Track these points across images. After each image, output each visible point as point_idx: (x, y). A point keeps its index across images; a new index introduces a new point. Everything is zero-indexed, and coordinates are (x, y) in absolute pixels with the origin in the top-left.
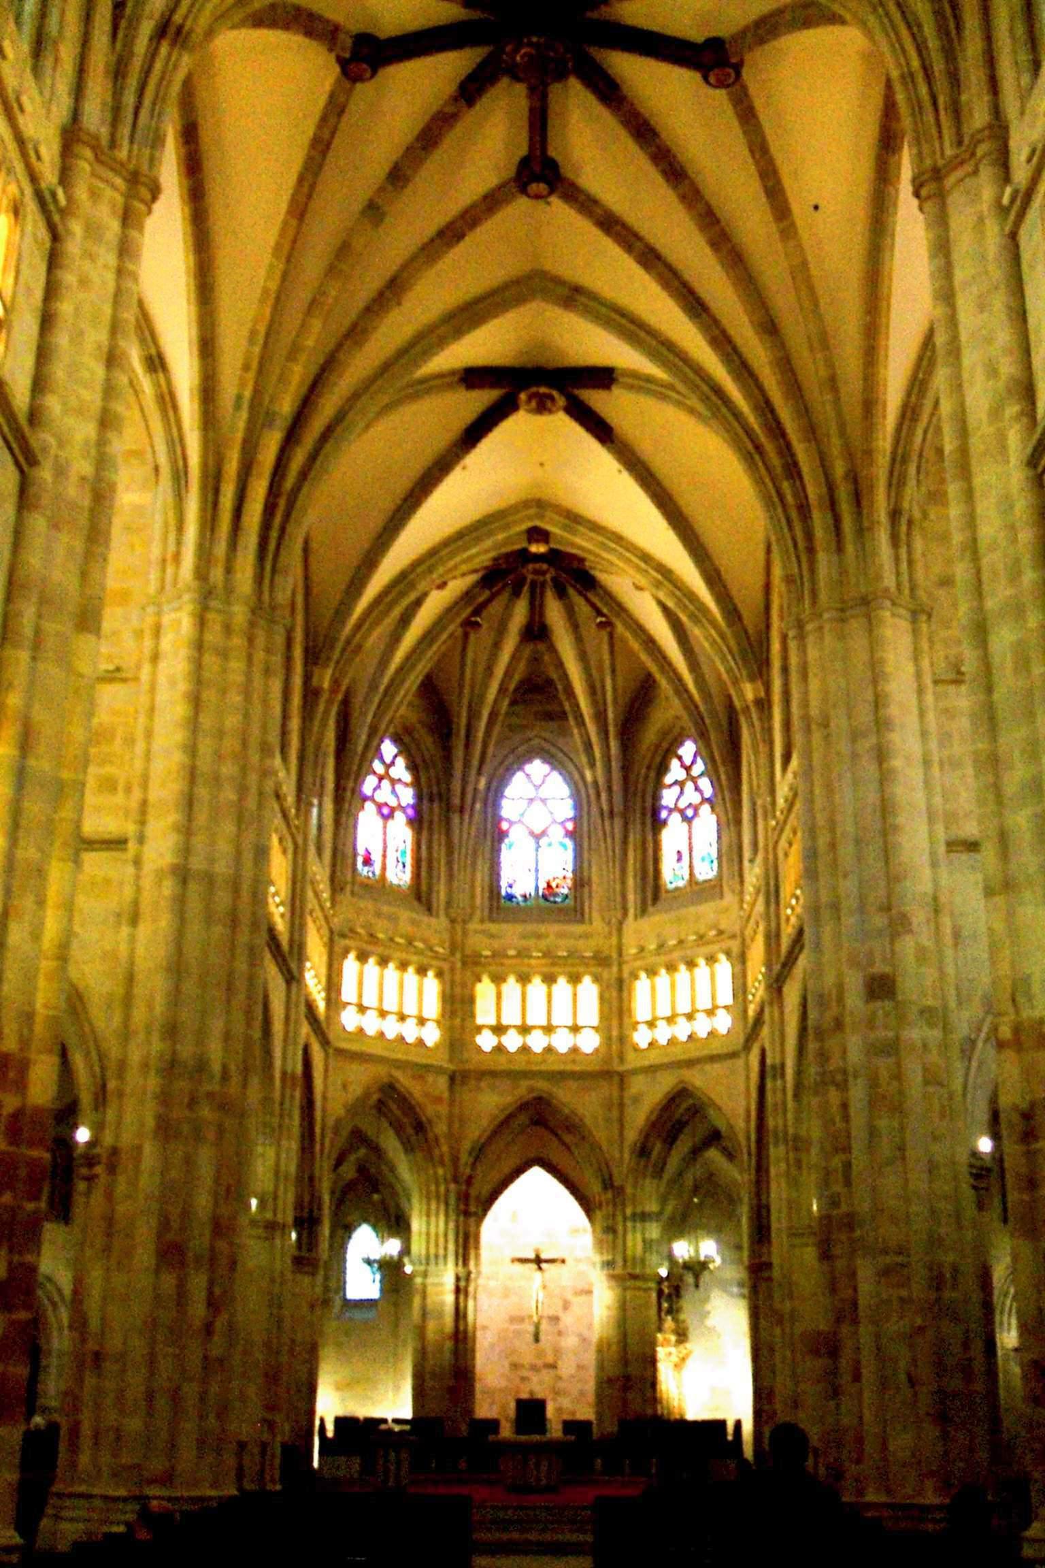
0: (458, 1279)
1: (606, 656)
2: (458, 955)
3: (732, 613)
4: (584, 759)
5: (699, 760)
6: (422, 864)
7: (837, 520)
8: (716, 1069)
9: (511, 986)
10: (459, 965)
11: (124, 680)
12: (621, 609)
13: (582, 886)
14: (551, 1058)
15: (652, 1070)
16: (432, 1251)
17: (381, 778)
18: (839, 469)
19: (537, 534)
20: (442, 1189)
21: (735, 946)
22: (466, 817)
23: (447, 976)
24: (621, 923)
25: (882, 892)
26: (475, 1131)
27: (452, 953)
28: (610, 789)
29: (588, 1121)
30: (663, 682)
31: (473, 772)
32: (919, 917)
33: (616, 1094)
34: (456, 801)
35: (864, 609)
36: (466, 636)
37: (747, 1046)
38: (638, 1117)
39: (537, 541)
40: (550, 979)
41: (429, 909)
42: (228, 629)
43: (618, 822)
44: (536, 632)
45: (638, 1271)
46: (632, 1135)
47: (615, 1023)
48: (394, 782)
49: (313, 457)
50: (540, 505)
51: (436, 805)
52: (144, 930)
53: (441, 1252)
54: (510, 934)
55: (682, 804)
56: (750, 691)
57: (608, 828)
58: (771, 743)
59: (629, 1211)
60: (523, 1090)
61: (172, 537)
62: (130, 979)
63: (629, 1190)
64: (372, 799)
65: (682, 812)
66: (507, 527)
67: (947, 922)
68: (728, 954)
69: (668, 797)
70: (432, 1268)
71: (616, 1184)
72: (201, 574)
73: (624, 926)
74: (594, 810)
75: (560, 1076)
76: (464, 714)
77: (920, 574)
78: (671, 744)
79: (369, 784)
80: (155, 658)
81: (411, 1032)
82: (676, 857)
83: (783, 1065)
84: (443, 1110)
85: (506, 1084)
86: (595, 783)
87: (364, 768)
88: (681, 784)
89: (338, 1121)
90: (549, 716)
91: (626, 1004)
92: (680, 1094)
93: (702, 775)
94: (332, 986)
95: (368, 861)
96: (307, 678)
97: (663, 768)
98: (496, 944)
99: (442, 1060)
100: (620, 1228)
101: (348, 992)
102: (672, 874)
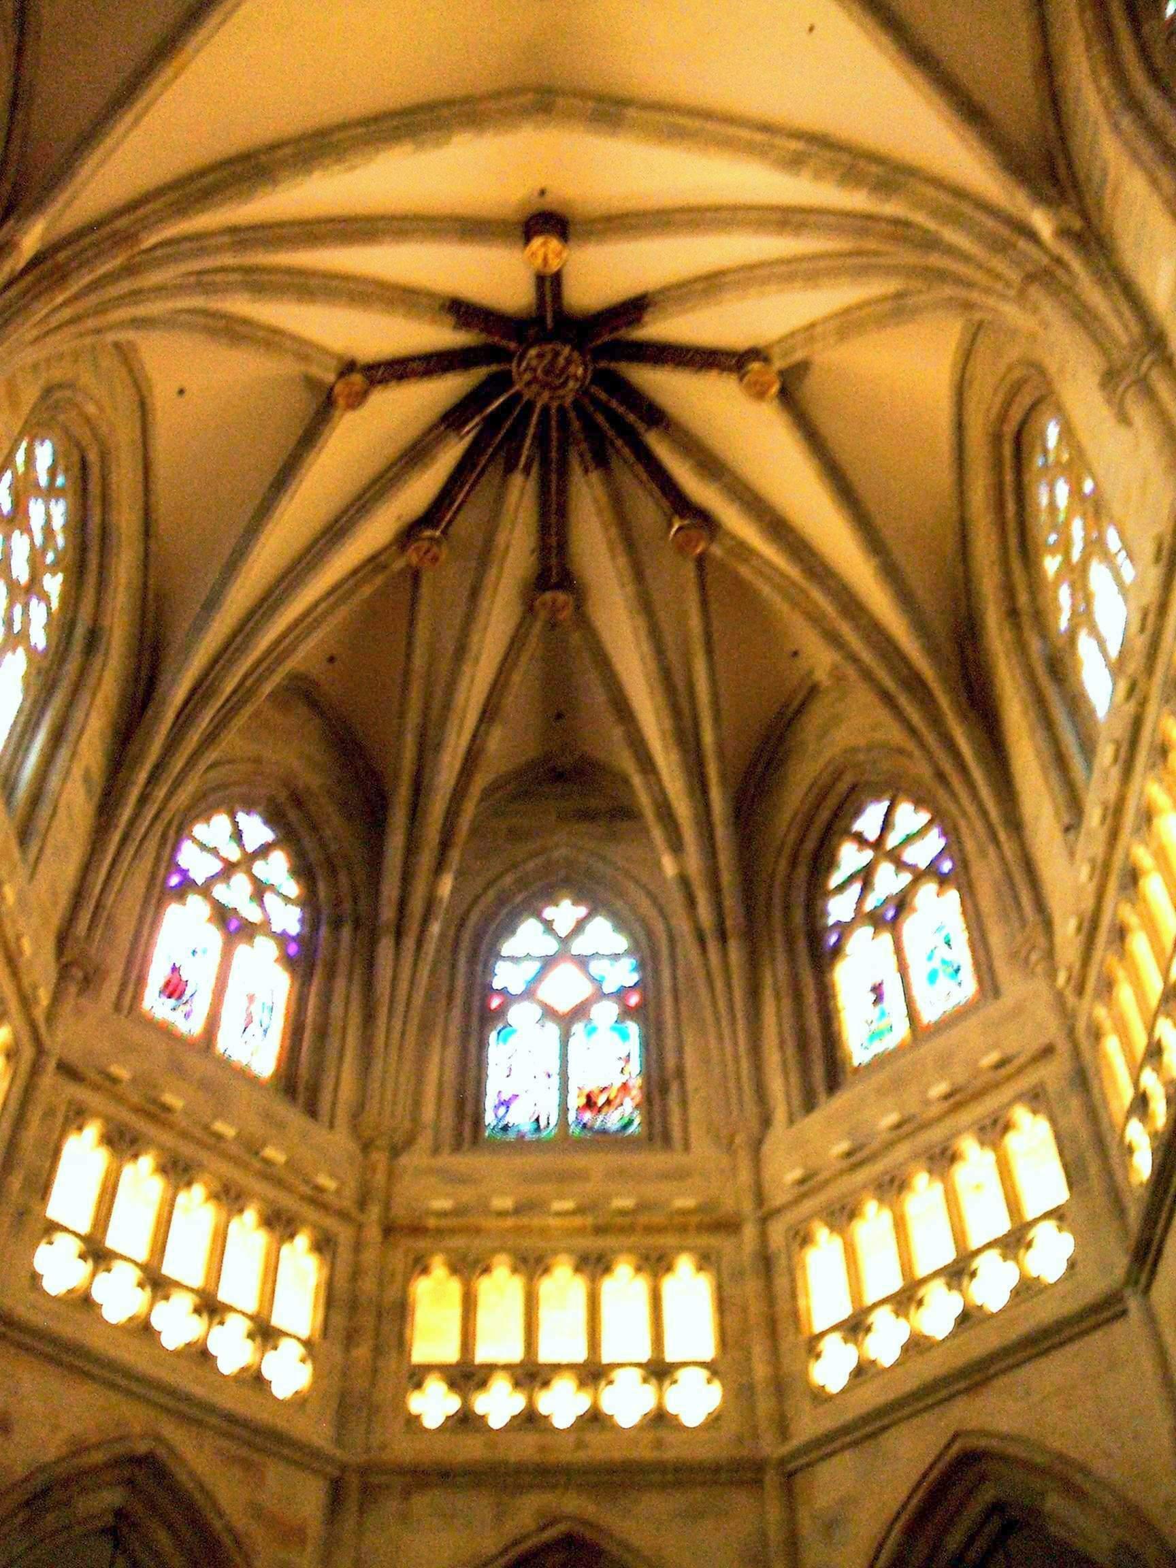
1: (695, 623)
2: (375, 1211)
10: (373, 1233)
13: (664, 1089)
21: (1052, 1073)
22: (409, 943)
24: (757, 1145)
28: (716, 889)
31: (426, 858)
33: (774, 1513)
34: (388, 914)
41: (312, 1111)
47: (759, 1350)
48: (260, 890)
51: (346, 932)
55: (869, 905)
68: (1036, 1099)
69: (839, 908)
73: (766, 1148)
74: (683, 926)
76: (410, 740)
78: (836, 815)
82: (873, 997)
85: (481, 1505)
86: (684, 881)
88: (866, 876)
91: (783, 1306)
95: (174, 989)
97: (824, 860)
98: (467, 1194)
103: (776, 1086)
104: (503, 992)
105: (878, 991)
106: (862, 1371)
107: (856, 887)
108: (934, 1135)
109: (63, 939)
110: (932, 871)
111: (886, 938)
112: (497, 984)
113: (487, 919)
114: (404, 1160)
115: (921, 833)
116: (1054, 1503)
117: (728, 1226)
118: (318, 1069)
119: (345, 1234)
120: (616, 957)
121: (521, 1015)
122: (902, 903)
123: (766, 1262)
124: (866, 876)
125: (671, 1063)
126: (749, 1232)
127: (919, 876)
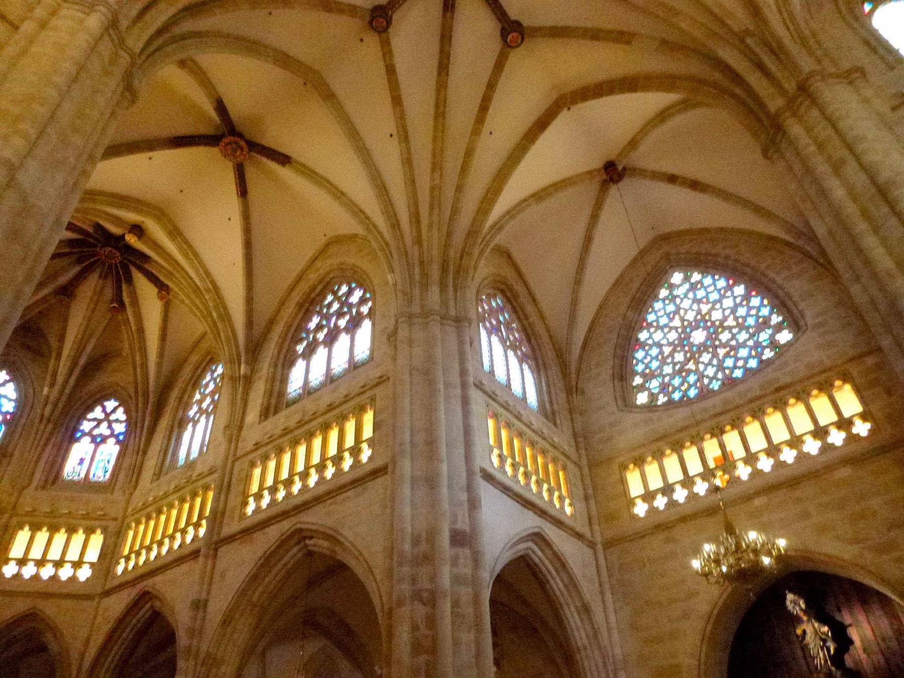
8: (67, 604)
19: (138, 230)
28: (55, 406)
43: (50, 426)
55: (95, 432)
65: (94, 439)
68: (105, 531)
69: (86, 426)
86: (48, 397)
88: (99, 422)
97: (91, 409)
103: (37, 476)
105: (82, 461)
106: (17, 576)
107: (95, 423)
108: (75, 522)
110: (117, 436)
111: (93, 446)
115: (121, 422)
120: (10, 400)
122: (104, 439)
124: (99, 422)
127: (112, 435)
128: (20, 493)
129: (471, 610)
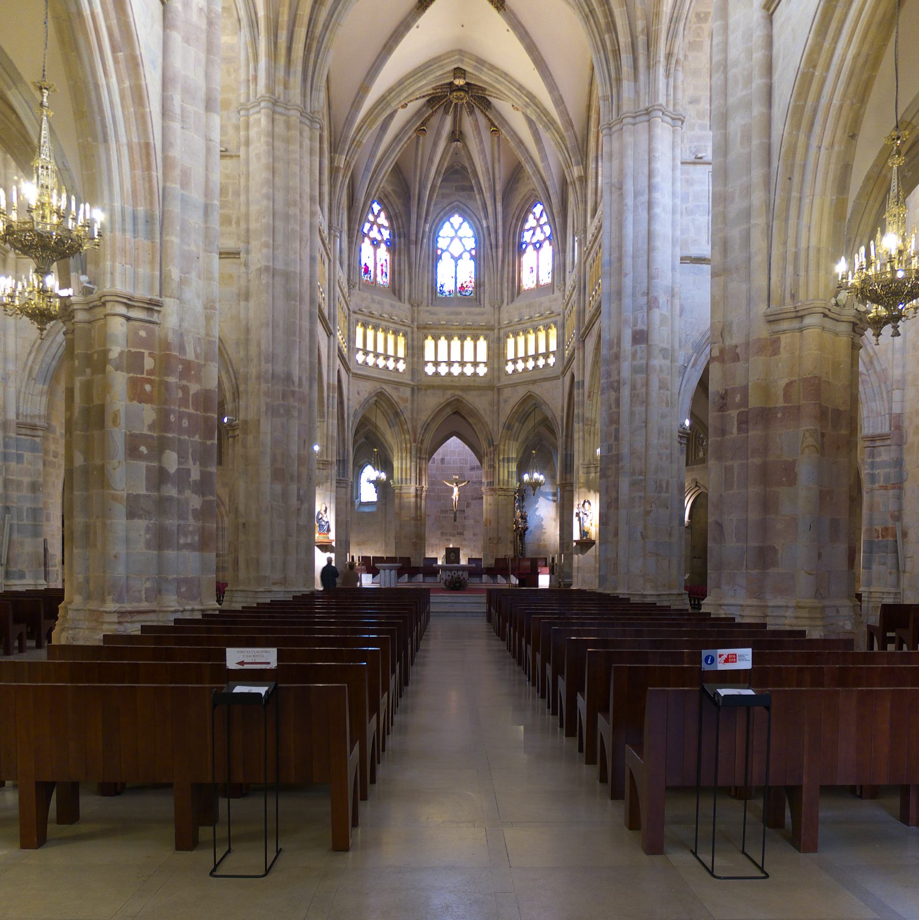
0: (417, 490)
2: (416, 324)
3: (569, 123)
4: (482, 214)
5: (544, 214)
6: (395, 273)
7: (635, 60)
8: (547, 385)
9: (443, 342)
10: (415, 329)
11: (231, 157)
12: (504, 122)
13: (480, 286)
14: (462, 379)
15: (514, 385)
16: (404, 477)
17: (372, 224)
18: (640, 25)
19: (459, 72)
20: (409, 446)
21: (559, 319)
23: (410, 335)
24: (500, 307)
25: (645, 285)
26: (424, 417)
27: (412, 322)
29: (482, 412)
30: (528, 168)
32: (662, 299)
33: (496, 396)
34: (413, 238)
35: (645, 118)
36: (418, 137)
37: (563, 373)
38: (507, 410)
39: (459, 77)
40: (462, 338)
41: (400, 299)
42: (288, 127)
43: (500, 250)
44: (457, 135)
45: (505, 487)
46: (503, 419)
47: (496, 360)
49: (331, 15)
50: (461, 53)
52: (252, 304)
53: (408, 477)
54: (441, 314)
55: (534, 241)
56: (576, 171)
57: (494, 254)
58: (586, 202)
59: (501, 458)
60: (449, 394)
61: (251, 65)
62: (248, 330)
63: (502, 447)
64: (366, 235)
65: (534, 245)
66: (442, 67)
67: (677, 302)
68: (555, 324)
69: (527, 237)
70: (404, 485)
71: (495, 444)
72: (270, 89)
74: (487, 243)
75: (466, 388)
77: (680, 94)
79: (367, 226)
80: (247, 143)
81: (391, 364)
82: (530, 270)
83: (583, 381)
84: (409, 405)
86: (488, 227)
87: (363, 220)
88: (534, 228)
89: (356, 411)
90: (463, 189)
91: (501, 351)
92: (529, 397)
93: (545, 224)
94: (351, 339)
95: (367, 270)
96: (332, 161)
97: (525, 220)
99: (407, 379)
100: (497, 466)
101: (359, 344)
102: (528, 281)
104: (442, 249)
106: (515, 371)
109: (349, 280)
112: (439, 245)
113: (436, 227)
114: (420, 308)
116: (543, 407)
117: (491, 329)
118: (400, 285)
119: (409, 330)
121: (446, 256)
123: (499, 339)
125: (482, 280)
126: (496, 331)
128: (500, 309)
129: (644, 390)
